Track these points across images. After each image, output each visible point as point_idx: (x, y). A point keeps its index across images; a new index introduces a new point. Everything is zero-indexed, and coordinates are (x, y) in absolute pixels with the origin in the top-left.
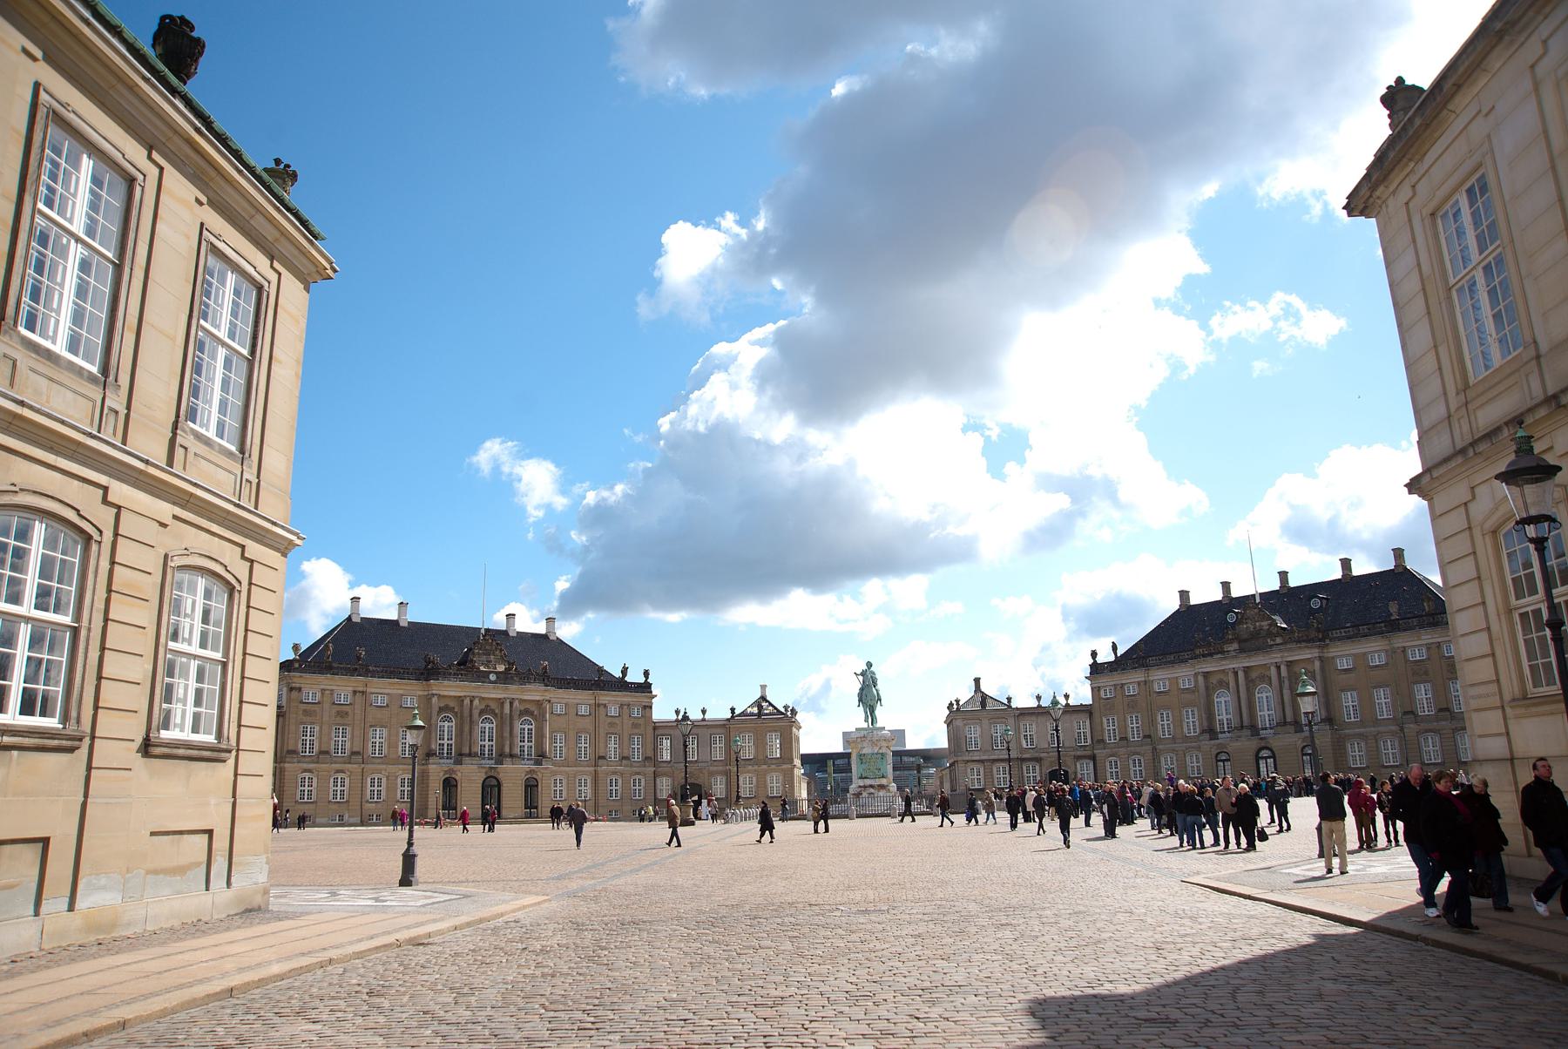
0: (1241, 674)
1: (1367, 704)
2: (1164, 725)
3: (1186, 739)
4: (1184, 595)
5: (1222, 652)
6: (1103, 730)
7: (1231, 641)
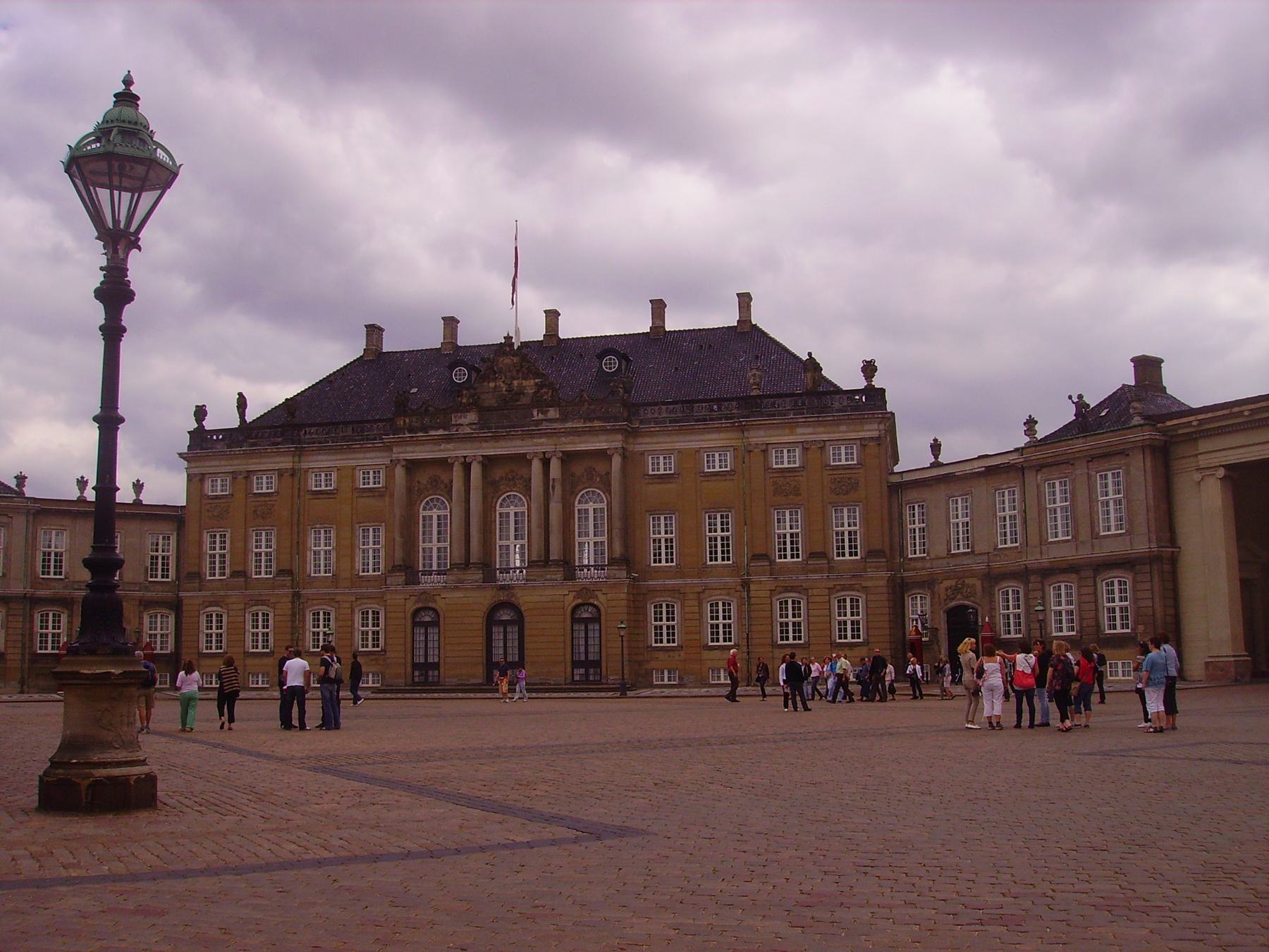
0: (476, 470)
2: (320, 550)
3: (357, 580)
6: (200, 556)
7: (465, 409)
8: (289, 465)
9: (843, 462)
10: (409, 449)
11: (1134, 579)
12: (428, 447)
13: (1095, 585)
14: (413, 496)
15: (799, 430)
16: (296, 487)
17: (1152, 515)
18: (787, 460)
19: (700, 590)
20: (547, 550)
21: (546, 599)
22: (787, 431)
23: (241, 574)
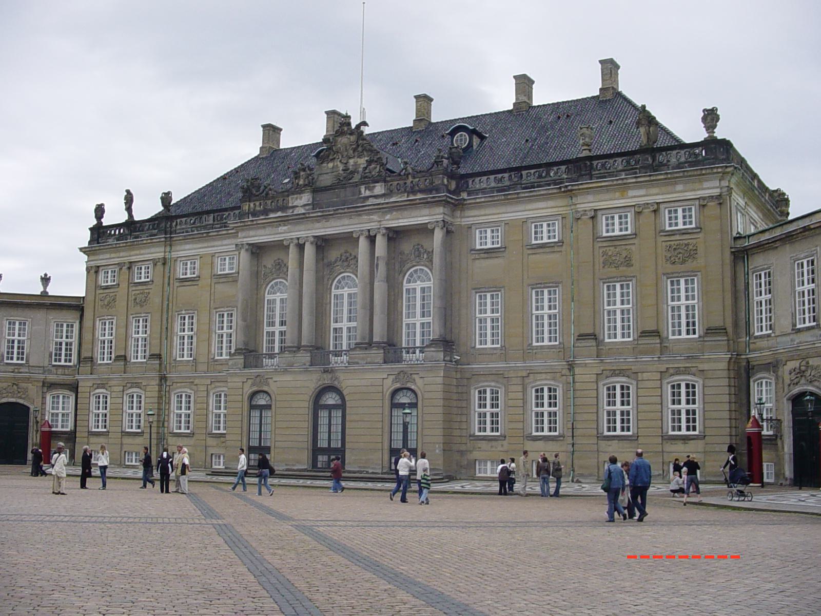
1: (516, 318)
4: (271, 132)
5: (284, 208)
7: (298, 190)
8: (161, 255)
9: (681, 226)
10: (252, 233)
12: (268, 230)
14: (258, 280)
15: (631, 193)
16: (167, 275)
18: (614, 228)
19: (525, 374)
20: (371, 330)
21: (366, 382)
22: (617, 194)
23: (123, 358)
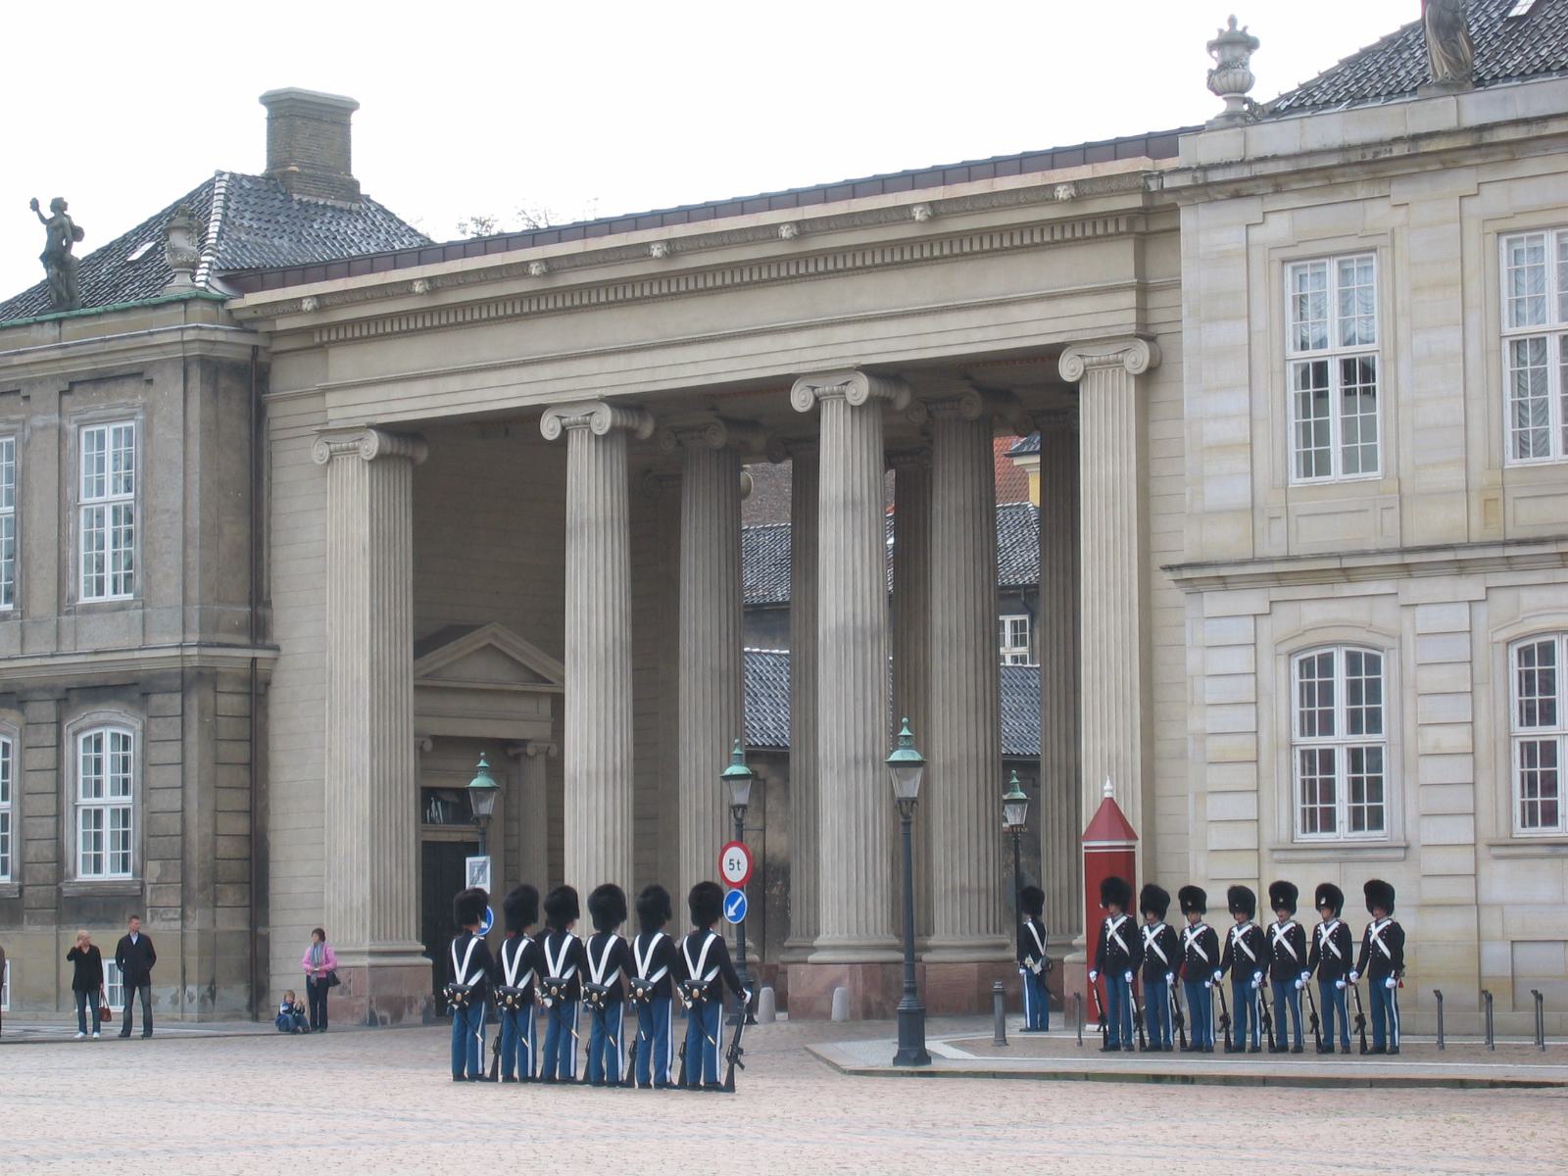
11: (145, 731)
13: (59, 745)
17: (194, 556)
